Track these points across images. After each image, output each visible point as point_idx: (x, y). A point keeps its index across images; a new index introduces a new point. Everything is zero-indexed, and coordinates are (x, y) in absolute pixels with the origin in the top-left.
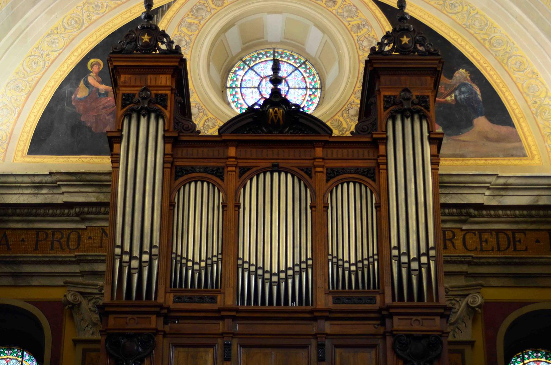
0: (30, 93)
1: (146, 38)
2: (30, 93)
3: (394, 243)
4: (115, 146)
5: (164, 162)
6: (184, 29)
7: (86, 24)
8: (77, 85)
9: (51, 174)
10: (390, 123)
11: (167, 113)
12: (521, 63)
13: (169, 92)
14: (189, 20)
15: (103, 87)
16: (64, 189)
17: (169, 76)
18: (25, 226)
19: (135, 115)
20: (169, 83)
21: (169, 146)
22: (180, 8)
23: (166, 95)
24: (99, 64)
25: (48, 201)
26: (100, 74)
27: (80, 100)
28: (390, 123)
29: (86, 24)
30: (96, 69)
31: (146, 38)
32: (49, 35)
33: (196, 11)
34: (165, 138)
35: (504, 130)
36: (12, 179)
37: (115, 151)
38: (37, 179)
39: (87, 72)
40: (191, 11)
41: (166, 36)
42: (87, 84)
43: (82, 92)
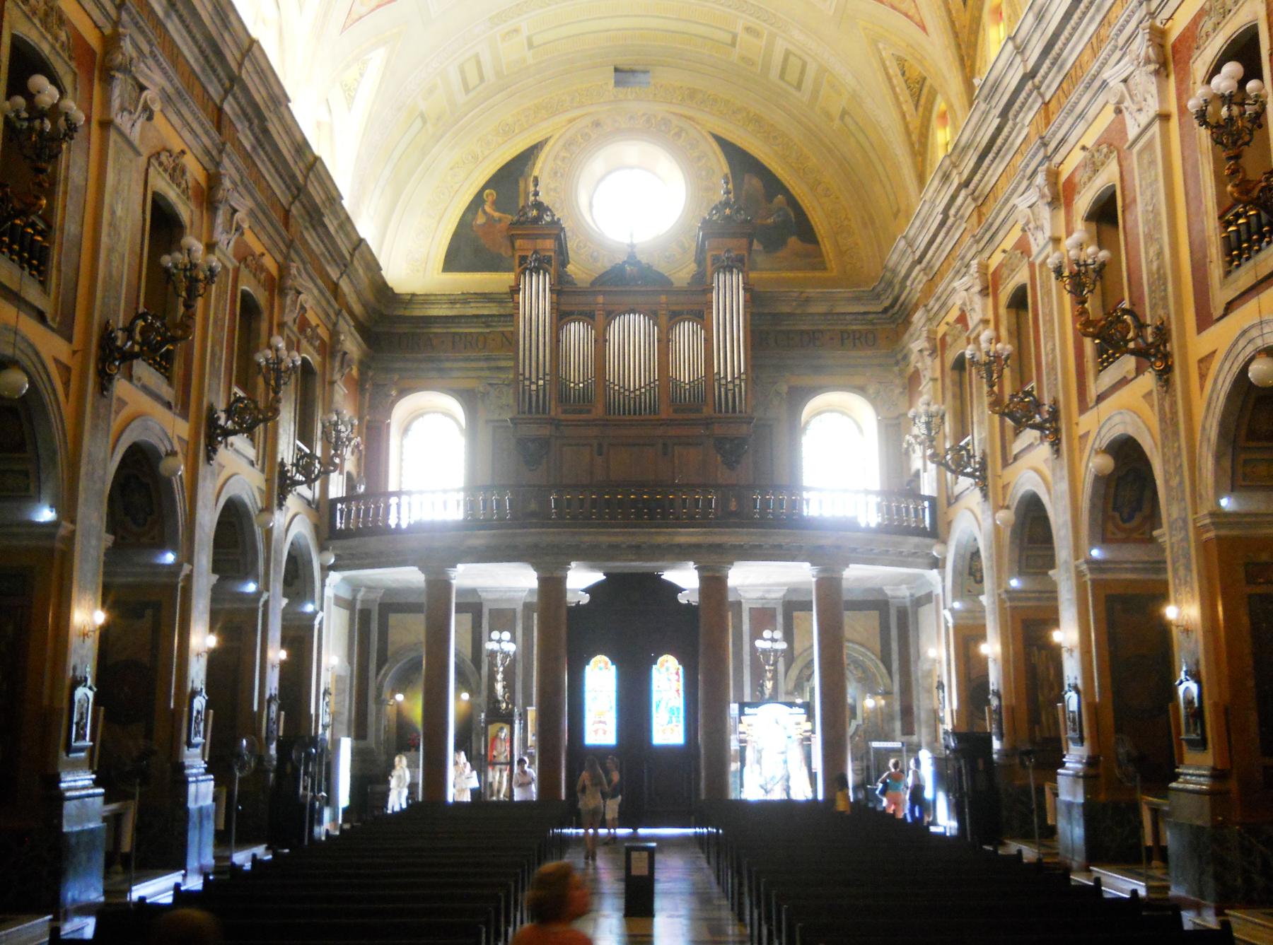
0: (441, 218)
1: (535, 213)
2: (441, 218)
3: (716, 371)
4: (516, 296)
5: (552, 309)
6: (559, 163)
7: (480, 159)
8: (476, 213)
9: (463, 294)
10: (716, 275)
11: (552, 271)
12: (828, 189)
13: (552, 254)
14: (563, 154)
15: (497, 215)
16: (472, 305)
17: (552, 241)
18: (445, 331)
19: (527, 273)
20: (552, 247)
21: (554, 296)
22: (555, 143)
23: (551, 257)
24: (492, 194)
25: (461, 313)
26: (494, 203)
27: (479, 225)
28: (716, 275)
29: (480, 159)
30: (490, 198)
31: (535, 213)
32: (451, 169)
33: (569, 145)
34: (551, 290)
35: (810, 247)
36: (433, 298)
37: (516, 300)
38: (452, 297)
39: (483, 202)
40: (564, 146)
41: (550, 210)
42: (485, 212)
43: (481, 220)
